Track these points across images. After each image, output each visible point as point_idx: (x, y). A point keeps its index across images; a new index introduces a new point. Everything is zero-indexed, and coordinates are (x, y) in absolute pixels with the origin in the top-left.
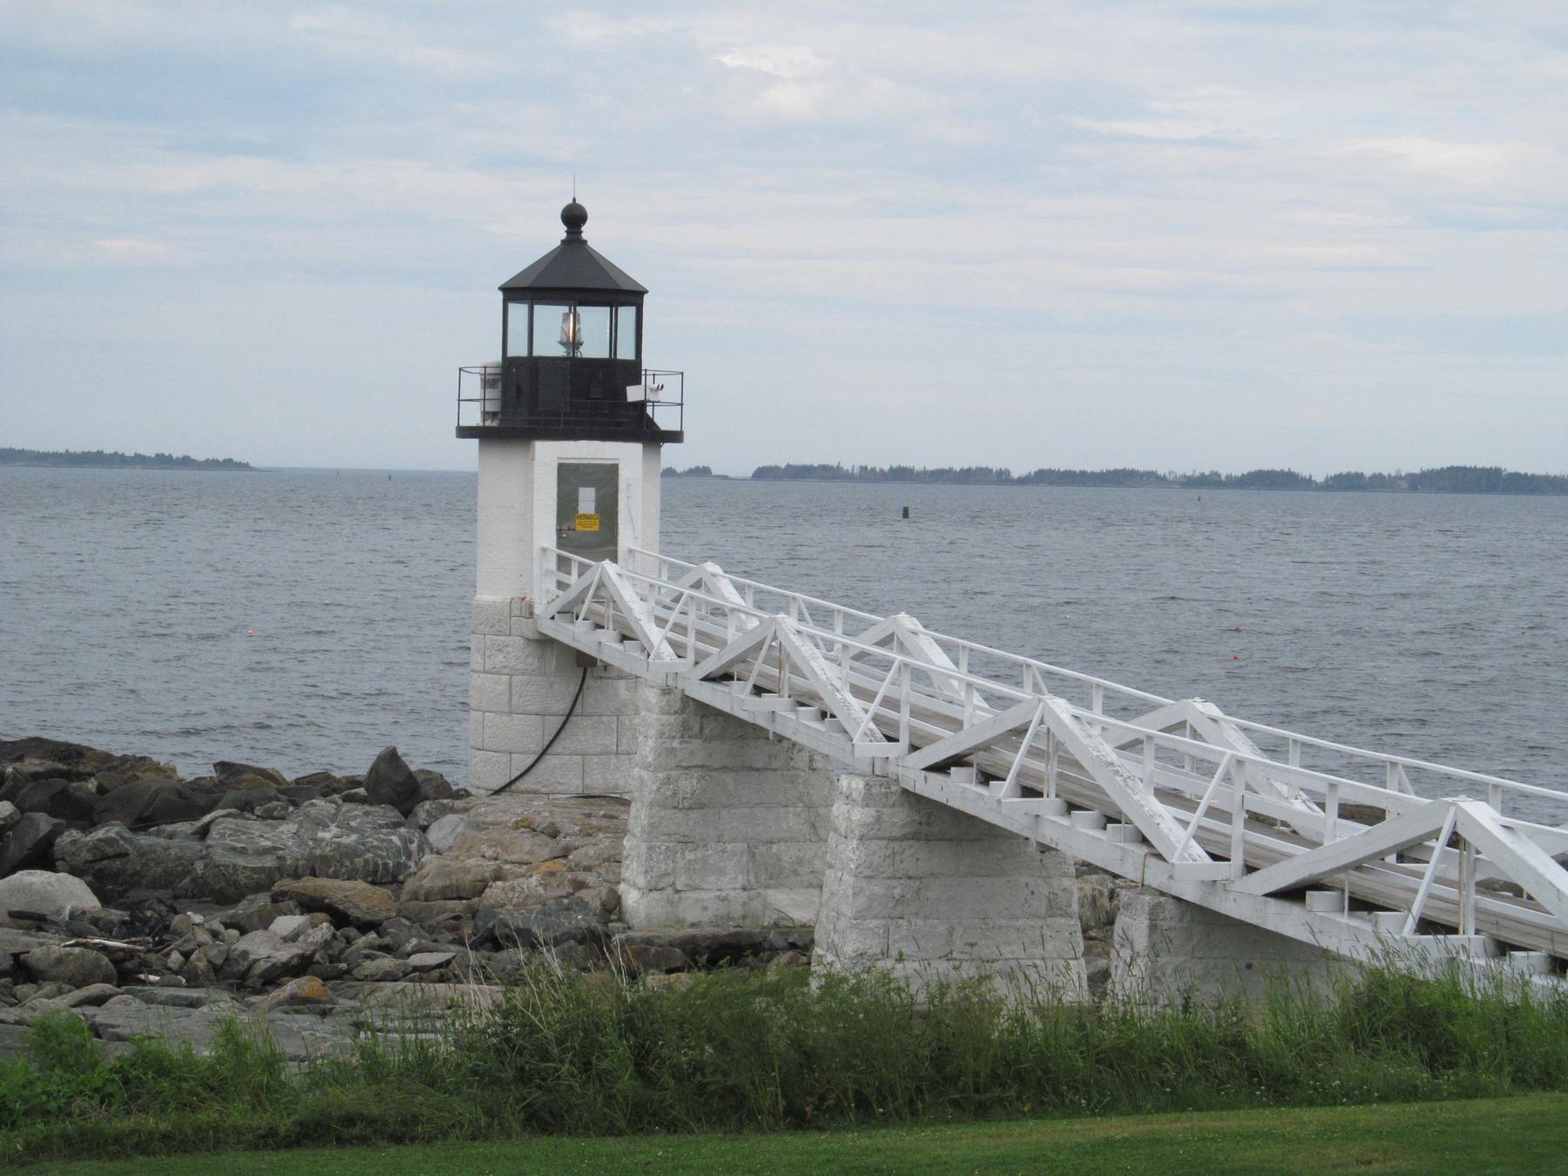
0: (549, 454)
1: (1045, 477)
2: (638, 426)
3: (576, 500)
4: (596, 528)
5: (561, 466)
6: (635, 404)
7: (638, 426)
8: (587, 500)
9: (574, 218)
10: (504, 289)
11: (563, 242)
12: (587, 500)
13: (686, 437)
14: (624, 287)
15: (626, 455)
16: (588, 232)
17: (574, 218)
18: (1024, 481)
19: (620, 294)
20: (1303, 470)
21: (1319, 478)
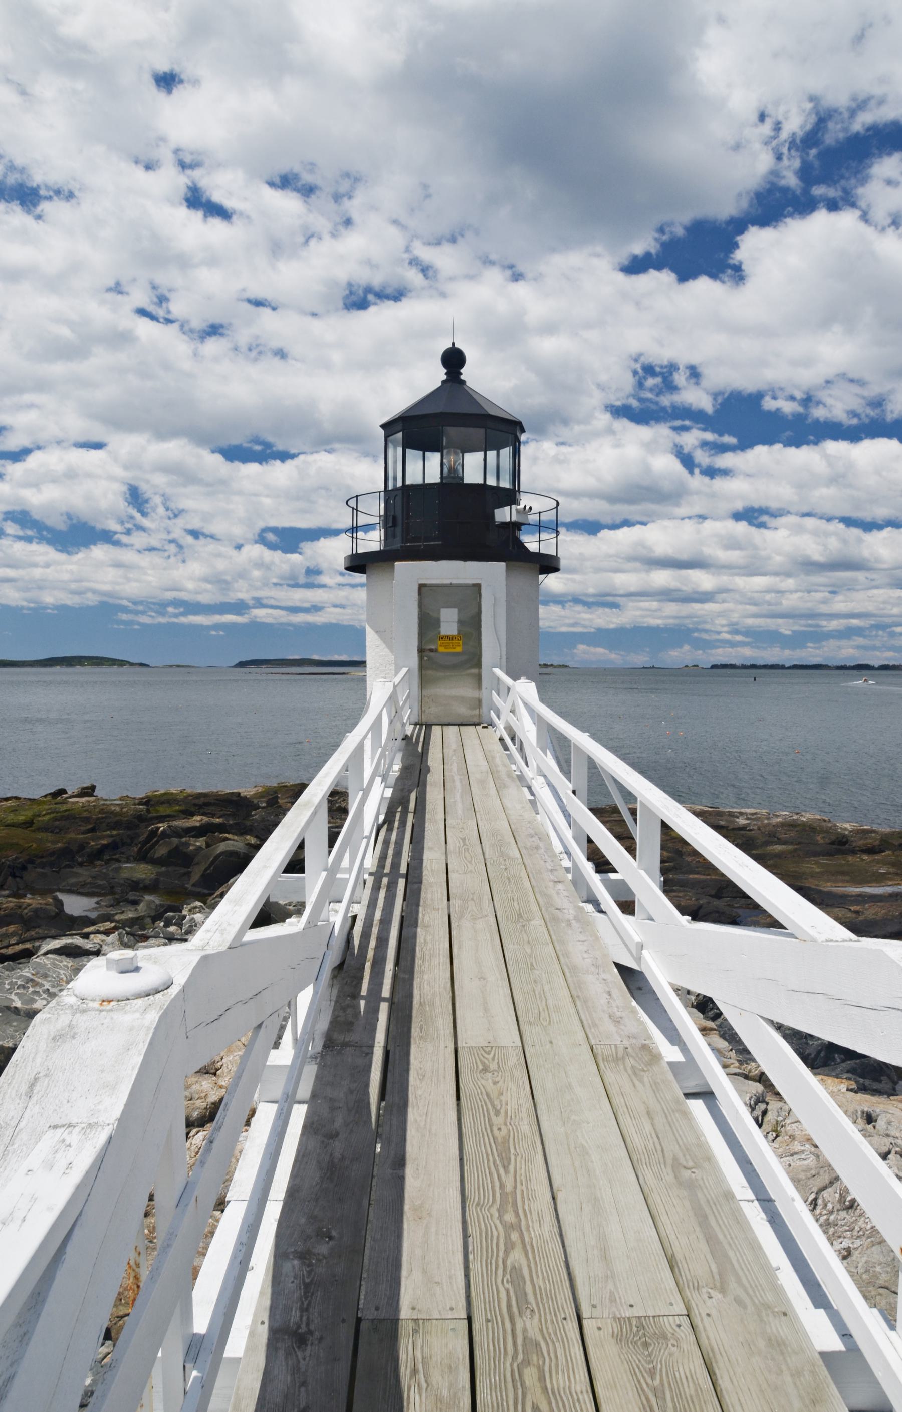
0: (410, 573)
1: (795, 667)
2: (505, 546)
3: (437, 623)
4: (459, 649)
5: (421, 587)
6: (505, 525)
7: (505, 546)
8: (449, 622)
9: (453, 360)
10: (383, 426)
11: (444, 382)
12: (449, 622)
13: (563, 563)
14: (492, 412)
15: (489, 575)
16: (466, 373)
17: (453, 360)
18: (789, 668)
19: (503, 431)
20: (871, 663)
21: (876, 666)
